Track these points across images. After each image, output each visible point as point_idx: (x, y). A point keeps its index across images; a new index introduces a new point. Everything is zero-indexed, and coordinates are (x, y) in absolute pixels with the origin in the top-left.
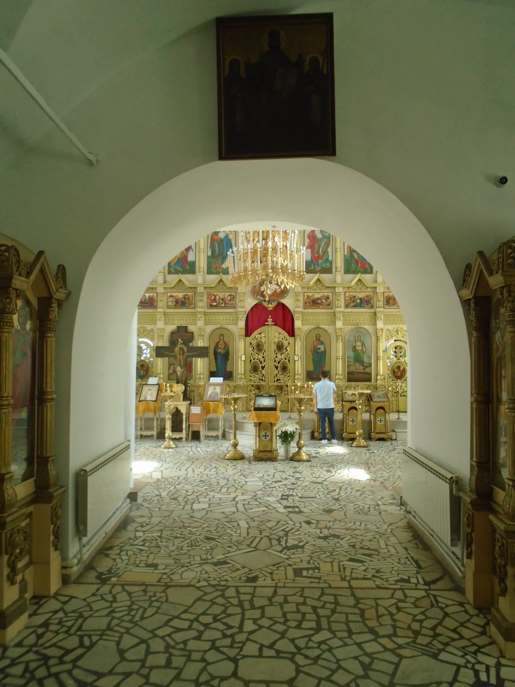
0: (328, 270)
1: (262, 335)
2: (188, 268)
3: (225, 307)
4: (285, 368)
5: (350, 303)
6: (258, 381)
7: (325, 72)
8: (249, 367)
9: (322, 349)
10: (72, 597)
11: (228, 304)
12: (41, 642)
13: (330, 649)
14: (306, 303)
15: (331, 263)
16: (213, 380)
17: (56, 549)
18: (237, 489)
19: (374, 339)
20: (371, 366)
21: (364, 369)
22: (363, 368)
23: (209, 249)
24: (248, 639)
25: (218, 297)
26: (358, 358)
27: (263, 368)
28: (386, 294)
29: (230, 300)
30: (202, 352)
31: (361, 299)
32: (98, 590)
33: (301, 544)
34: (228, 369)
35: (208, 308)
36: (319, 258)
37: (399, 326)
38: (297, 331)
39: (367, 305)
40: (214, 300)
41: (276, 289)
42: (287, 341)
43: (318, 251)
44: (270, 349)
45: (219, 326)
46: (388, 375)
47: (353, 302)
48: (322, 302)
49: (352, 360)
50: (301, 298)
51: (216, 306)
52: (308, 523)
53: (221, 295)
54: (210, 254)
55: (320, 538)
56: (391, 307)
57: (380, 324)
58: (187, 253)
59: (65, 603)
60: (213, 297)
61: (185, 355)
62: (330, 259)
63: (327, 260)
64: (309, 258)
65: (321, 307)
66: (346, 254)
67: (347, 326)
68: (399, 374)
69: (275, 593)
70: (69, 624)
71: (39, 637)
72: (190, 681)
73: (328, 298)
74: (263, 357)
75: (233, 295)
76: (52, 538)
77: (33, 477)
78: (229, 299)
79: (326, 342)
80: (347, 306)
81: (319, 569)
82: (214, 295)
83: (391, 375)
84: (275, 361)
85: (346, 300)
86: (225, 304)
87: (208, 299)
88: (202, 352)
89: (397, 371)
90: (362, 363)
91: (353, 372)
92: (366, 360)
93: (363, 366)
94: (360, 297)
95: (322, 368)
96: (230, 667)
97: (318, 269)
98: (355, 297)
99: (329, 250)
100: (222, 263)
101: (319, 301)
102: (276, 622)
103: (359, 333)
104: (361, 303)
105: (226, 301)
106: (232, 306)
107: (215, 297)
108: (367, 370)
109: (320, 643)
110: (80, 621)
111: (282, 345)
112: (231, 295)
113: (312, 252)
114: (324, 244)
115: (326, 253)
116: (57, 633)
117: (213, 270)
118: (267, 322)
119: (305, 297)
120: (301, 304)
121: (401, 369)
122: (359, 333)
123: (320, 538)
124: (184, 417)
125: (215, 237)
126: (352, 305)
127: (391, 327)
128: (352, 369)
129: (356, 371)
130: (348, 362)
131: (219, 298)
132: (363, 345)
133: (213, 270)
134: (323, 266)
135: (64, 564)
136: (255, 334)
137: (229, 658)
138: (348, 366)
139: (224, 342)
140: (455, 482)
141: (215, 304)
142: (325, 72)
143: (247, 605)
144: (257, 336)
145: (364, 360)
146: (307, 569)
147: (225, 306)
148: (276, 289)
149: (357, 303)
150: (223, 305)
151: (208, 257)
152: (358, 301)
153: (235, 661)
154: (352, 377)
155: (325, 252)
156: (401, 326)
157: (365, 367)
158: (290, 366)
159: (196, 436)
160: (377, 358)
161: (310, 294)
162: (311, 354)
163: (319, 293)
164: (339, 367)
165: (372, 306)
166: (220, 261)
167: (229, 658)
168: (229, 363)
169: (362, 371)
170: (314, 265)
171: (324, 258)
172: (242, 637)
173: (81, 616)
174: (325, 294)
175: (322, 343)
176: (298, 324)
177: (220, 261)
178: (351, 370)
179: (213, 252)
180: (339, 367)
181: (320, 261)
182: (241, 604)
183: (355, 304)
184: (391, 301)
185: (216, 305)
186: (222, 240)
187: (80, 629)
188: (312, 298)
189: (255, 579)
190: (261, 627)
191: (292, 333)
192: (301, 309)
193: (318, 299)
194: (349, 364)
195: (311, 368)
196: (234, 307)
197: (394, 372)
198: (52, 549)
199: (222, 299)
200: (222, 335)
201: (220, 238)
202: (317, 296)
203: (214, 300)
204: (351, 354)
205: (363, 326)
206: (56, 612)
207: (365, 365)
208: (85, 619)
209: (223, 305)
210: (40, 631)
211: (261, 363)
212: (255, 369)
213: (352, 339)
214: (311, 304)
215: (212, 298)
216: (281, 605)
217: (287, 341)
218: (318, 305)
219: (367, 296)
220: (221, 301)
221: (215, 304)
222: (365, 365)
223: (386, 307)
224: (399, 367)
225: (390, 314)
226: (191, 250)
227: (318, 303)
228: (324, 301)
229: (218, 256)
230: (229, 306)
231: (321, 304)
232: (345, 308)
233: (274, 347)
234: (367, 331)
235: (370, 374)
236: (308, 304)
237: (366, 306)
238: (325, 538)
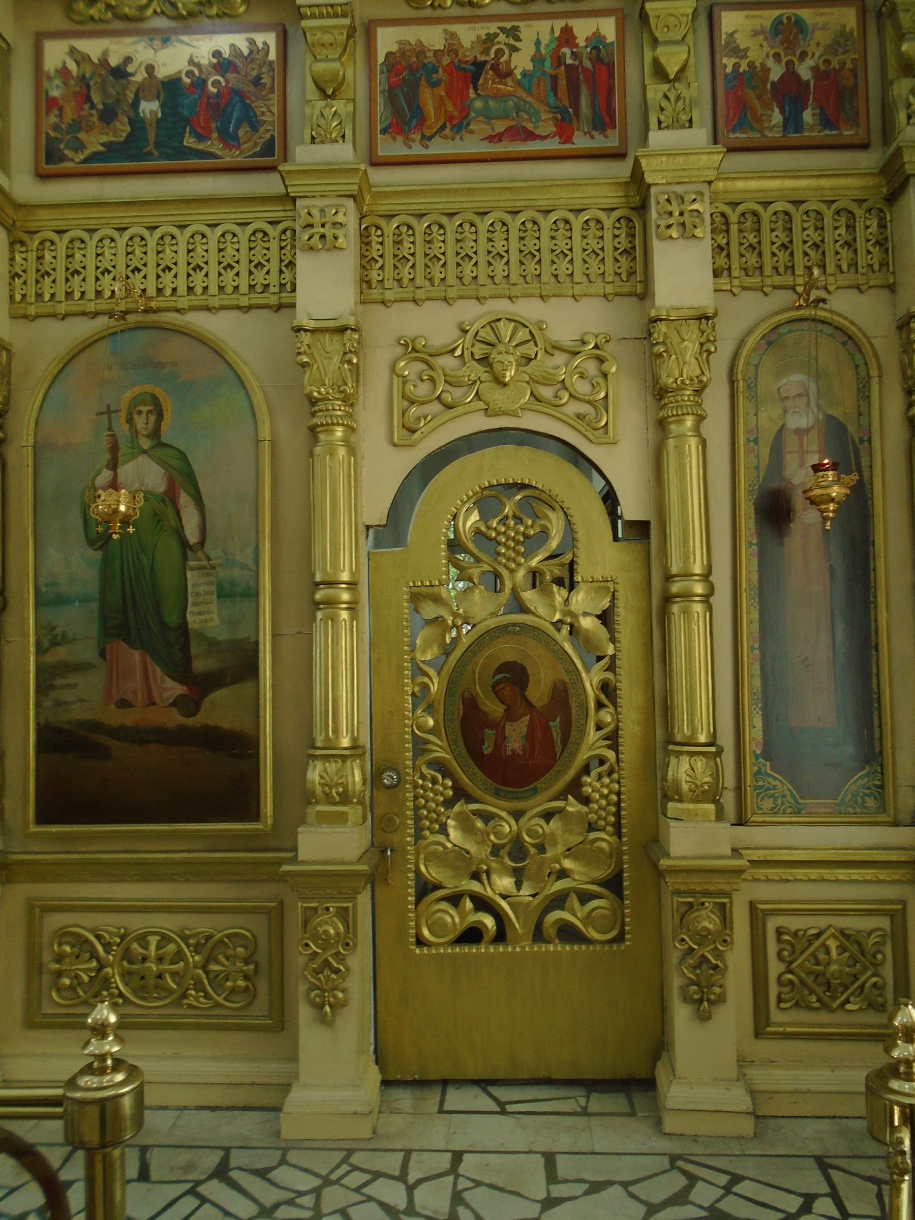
5: (77, 125)
19: (278, 425)
20: (251, 670)
21: (190, 704)
22: (173, 689)
26: (136, 602)
28: (387, 40)
37: (501, 306)
39: (229, 139)
46: (420, 747)
47: (108, 115)
49: (81, 623)
56: (437, 148)
57: (325, 287)
67: (52, 328)
68: (516, 736)
83: (440, 750)
85: (46, 104)
89: (494, 708)
90: (174, 645)
91: (95, 727)
92: (205, 617)
93: (181, 670)
94: (162, 73)
98: (120, 73)
108: (220, 710)
121: (538, 692)
126: (95, 142)
127: (436, 324)
128: (86, 699)
129: (115, 718)
132: (183, 477)
145: (193, 620)
149: (137, 123)
152: (150, 108)
156: (529, 309)
157: (200, 687)
160: (313, 599)
165: (268, 149)
169: (174, 719)
178: (78, 713)
183: (122, 129)
184: (428, 98)
194: (61, 653)
197: (469, 725)
205: (200, 321)
207: (200, 665)
219: (222, 65)
222: (200, 665)
223: (390, 147)
224: (514, 676)
225: (419, 203)
232: (43, 176)
234: (218, 353)
235: (243, 746)
237: (213, 145)
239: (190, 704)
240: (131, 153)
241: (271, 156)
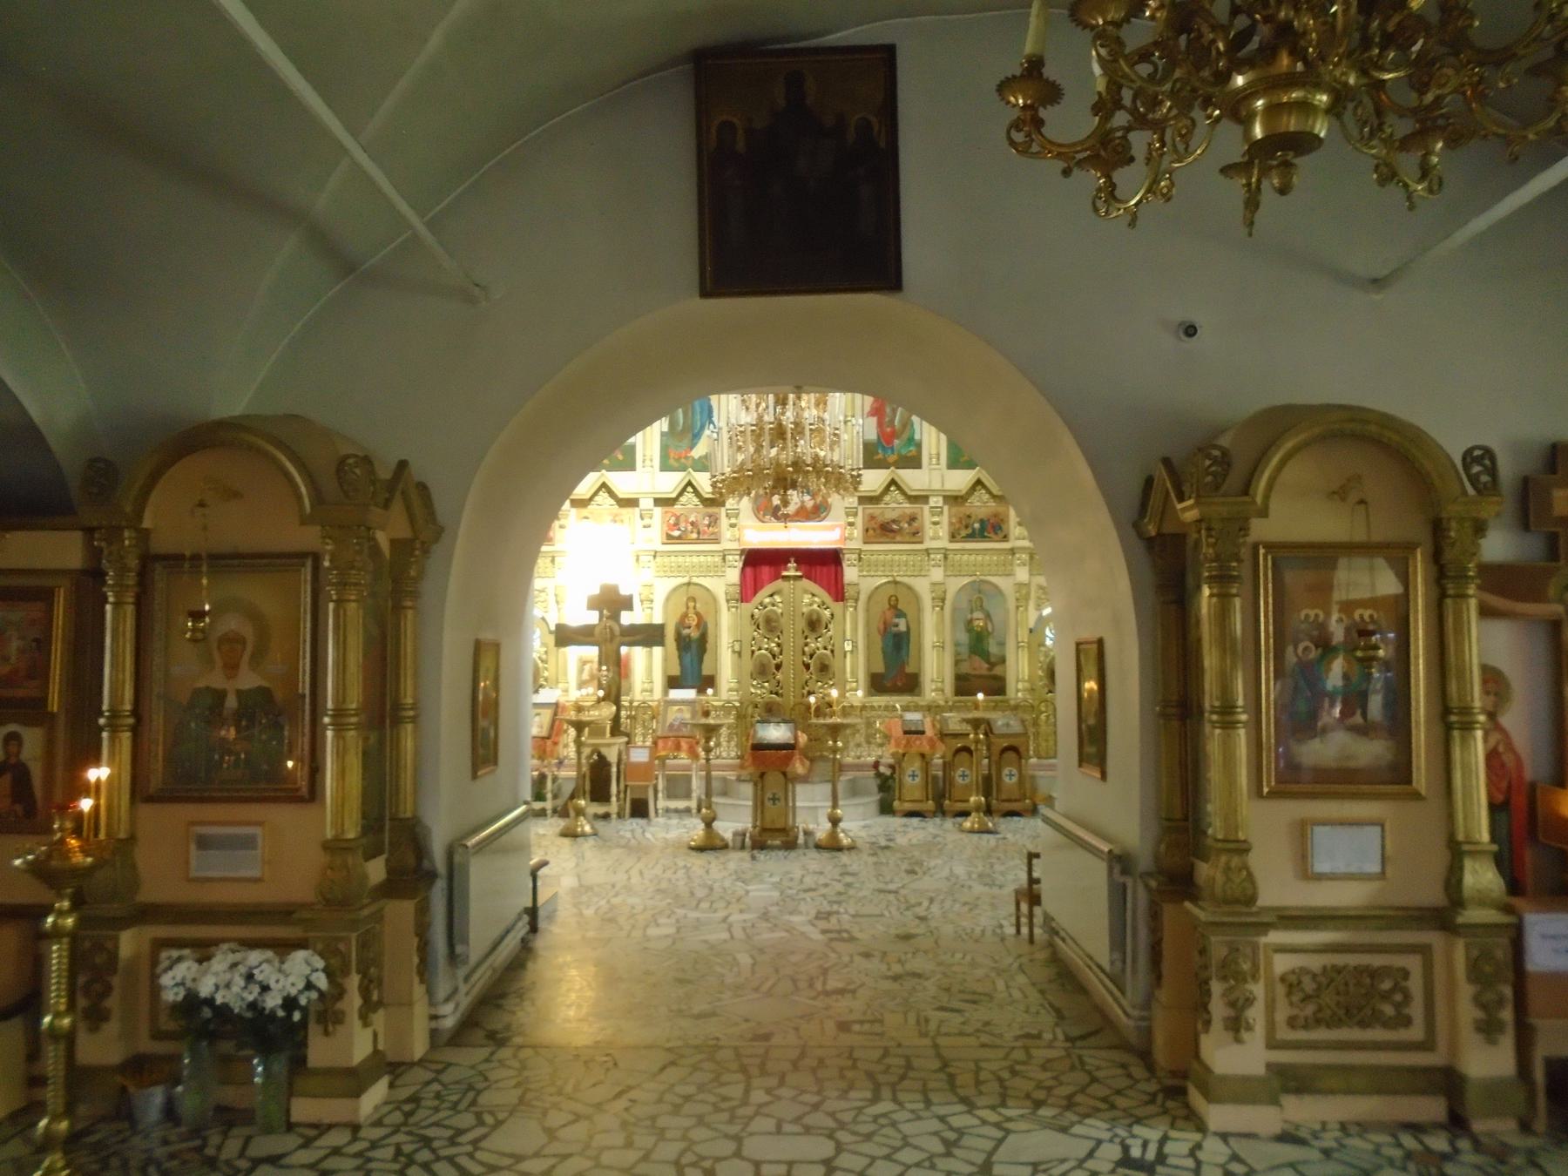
0: (914, 462)
1: (777, 598)
2: (620, 457)
3: (698, 541)
4: (824, 668)
6: (767, 695)
7: (882, 144)
8: (748, 665)
9: (902, 628)
10: (450, 1065)
12: (412, 1120)
13: (894, 1124)
15: (919, 446)
16: (675, 694)
17: (422, 981)
18: (729, 903)
19: (1011, 604)
24: (757, 1114)
25: (682, 519)
27: (778, 667)
30: (649, 635)
31: (982, 522)
32: (492, 1054)
33: (852, 987)
34: (706, 671)
36: (894, 435)
38: (849, 592)
42: (827, 613)
43: (892, 421)
44: (793, 629)
45: (686, 580)
49: (965, 651)
50: (859, 521)
51: (679, 538)
52: (867, 955)
55: (887, 978)
59: (439, 1072)
61: (618, 639)
62: (917, 437)
63: (911, 440)
64: (872, 435)
65: (898, 538)
69: (803, 1055)
70: (454, 1098)
71: (408, 1115)
72: (668, 1162)
73: (913, 519)
74: (779, 645)
76: (416, 960)
77: (381, 853)
79: (910, 613)
80: (953, 537)
81: (881, 1022)
84: (804, 653)
85: (951, 524)
88: (649, 635)
90: (985, 655)
92: (993, 649)
93: (988, 662)
94: (981, 516)
95: (903, 665)
96: (730, 1147)
97: (892, 458)
100: (691, 448)
102: (803, 1092)
103: (981, 594)
104: (983, 529)
107: (678, 518)
108: (997, 671)
109: (876, 1118)
110: (471, 1095)
111: (819, 620)
113: (880, 425)
116: (437, 1110)
118: (787, 569)
120: (857, 533)
122: (981, 594)
123: (887, 978)
124: (614, 769)
126: (964, 533)
128: (965, 668)
130: (957, 654)
132: (988, 616)
133: (672, 462)
134: (904, 452)
135: (433, 1012)
136: (763, 596)
137: (726, 1136)
138: (957, 663)
139: (697, 614)
140: (1120, 862)
141: (676, 533)
142: (882, 144)
143: (755, 1071)
144: (767, 600)
146: (862, 1022)
150: (694, 536)
151: (663, 434)
152: (977, 526)
153: (738, 1139)
154: (964, 685)
157: (992, 665)
158: (835, 664)
159: (640, 809)
162: (878, 640)
164: (935, 665)
166: (686, 442)
167: (726, 1136)
168: (706, 657)
169: (984, 672)
171: (905, 436)
172: (748, 1111)
173: (471, 1088)
174: (908, 512)
175: (900, 614)
176: (850, 574)
177: (686, 442)
180: (935, 665)
181: (896, 442)
182: (743, 1069)
183: (969, 531)
187: (474, 1103)
188: (880, 519)
189: (767, 1037)
190: (779, 1098)
191: (838, 591)
192: (856, 544)
193: (894, 521)
195: (879, 667)
196: (716, 541)
198: (416, 979)
199: (692, 524)
200: (694, 600)
202: (890, 515)
204: (964, 637)
206: (428, 1083)
208: (479, 1092)
209: (694, 536)
210: (407, 1108)
211: (774, 657)
212: (762, 671)
213: (965, 605)
216: (814, 1070)
217: (827, 613)
227: (893, 531)
229: (683, 431)
233: (801, 624)
238: (896, 978)
239: (990, 669)
240: (972, 536)
241: (1005, 538)
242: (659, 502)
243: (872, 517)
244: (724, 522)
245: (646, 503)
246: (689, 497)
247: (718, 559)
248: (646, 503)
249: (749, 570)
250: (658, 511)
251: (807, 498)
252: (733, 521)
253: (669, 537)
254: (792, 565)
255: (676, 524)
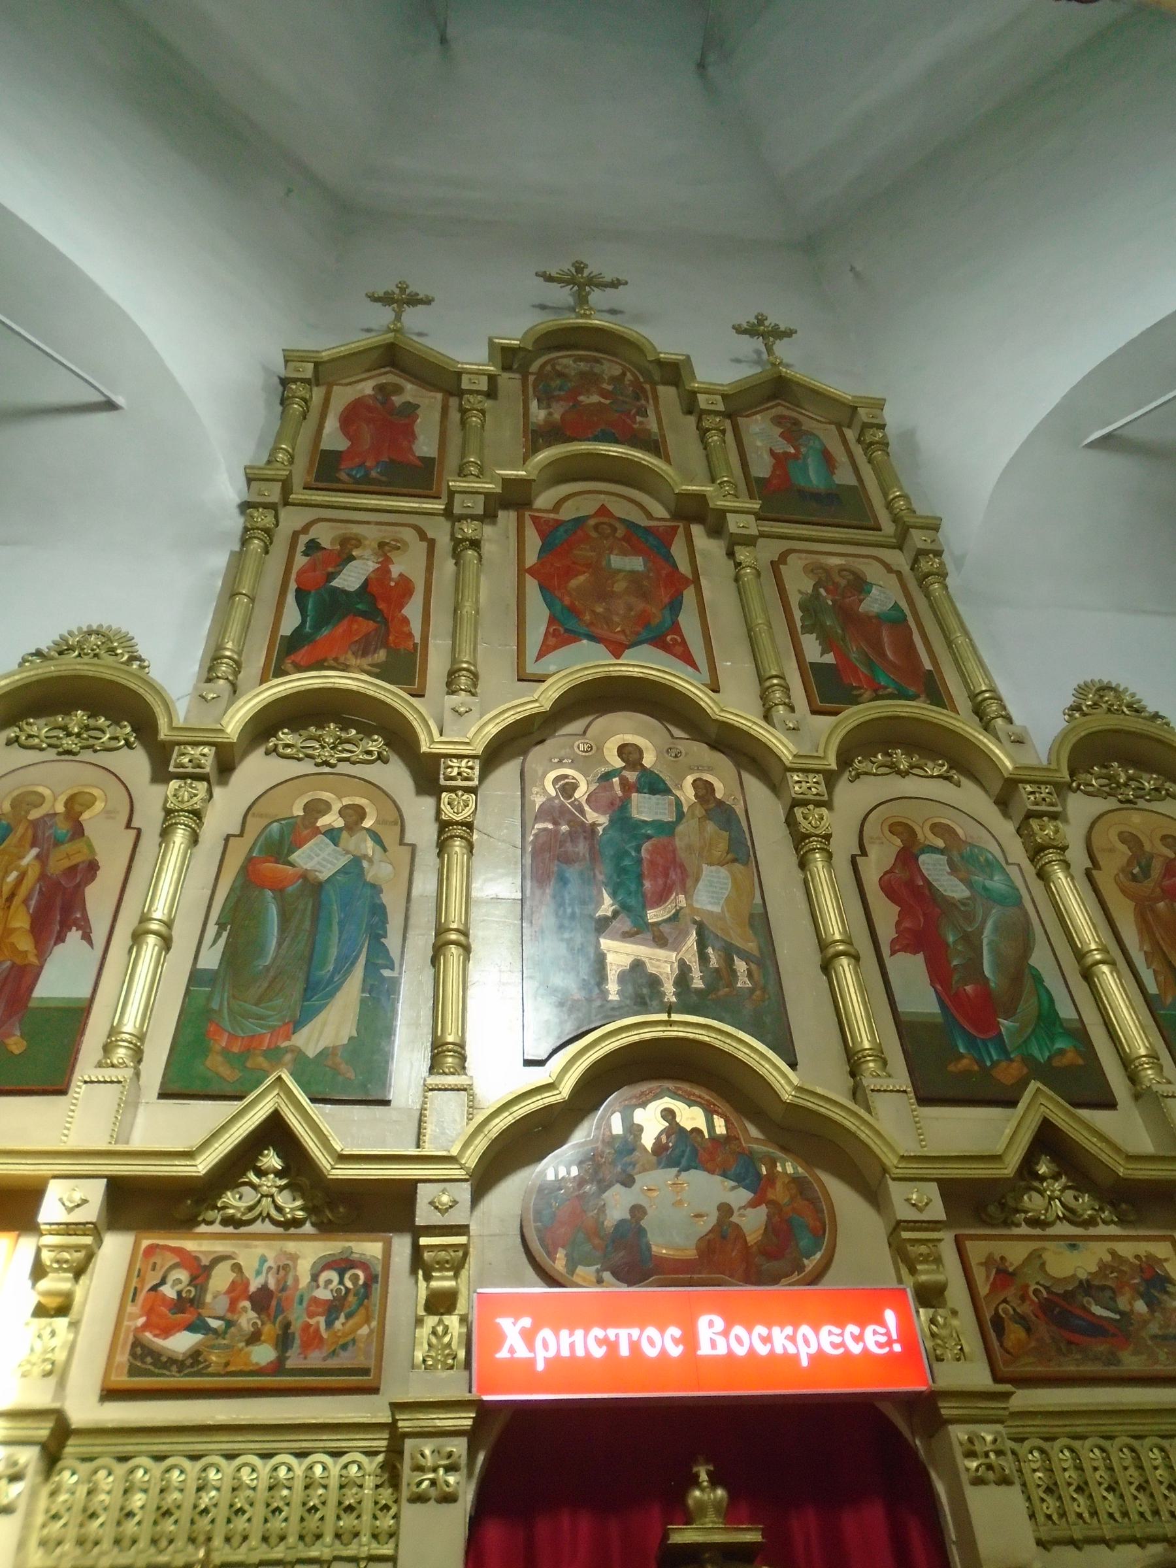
2: (16, 1044)
11: (312, 1339)
14: (998, 1324)
23: (212, 929)
25: (221, 1279)
29: (332, 1309)
35: (110, 1394)
40: (187, 1312)
41: (725, 1210)
48: (1121, 1313)
53: (256, 1258)
54: (211, 960)
58: (43, 953)
60: (183, 1275)
62: (1065, 1011)
63: (1048, 1020)
66: (1152, 989)
75: (364, 1265)
78: (324, 1294)
82: (187, 1260)
86: (284, 1341)
87: (130, 1294)
99: (1040, 959)
101: (1098, 1310)
105: (298, 1317)
106: (344, 1360)
107: (200, 1272)
112: (342, 1264)
113: (939, 973)
114: (996, 929)
115: (1028, 983)
117: (216, 1065)
119: (979, 1275)
125: (270, 867)
131: (238, 1289)
133: (216, 1065)
141: (181, 1342)
147: (277, 1368)
148: (725, 1210)
150: (263, 1354)
151: (196, 977)
155: (1021, 974)
161: (1016, 1254)
163: (1073, 1243)
170: (971, 1042)
171: (1028, 1006)
179: (237, 957)
181: (1006, 1025)
185: (195, 1355)
186: (314, 888)
193: (1086, 1287)
199: (262, 1300)
201: (304, 876)
203: (182, 1304)
214: (1043, 1329)
215: (169, 1291)
218: (1101, 1348)
220: (247, 1318)
221: (181, 1342)
226: (74, 935)
227: (1097, 1329)
228: (1140, 1306)
230: (315, 1359)
231: (1122, 1331)
236: (1016, 1333)
242: (143, 1202)
243: (1004, 1276)
244: (406, 1293)
245: (66, 1201)
246: (267, 1189)
247: (364, 1468)
248: (66, 1201)
249: (494, 1532)
250: (116, 1249)
251: (740, 1197)
252: (442, 1283)
253: (144, 1357)
254: (706, 1494)
255: (187, 1312)
